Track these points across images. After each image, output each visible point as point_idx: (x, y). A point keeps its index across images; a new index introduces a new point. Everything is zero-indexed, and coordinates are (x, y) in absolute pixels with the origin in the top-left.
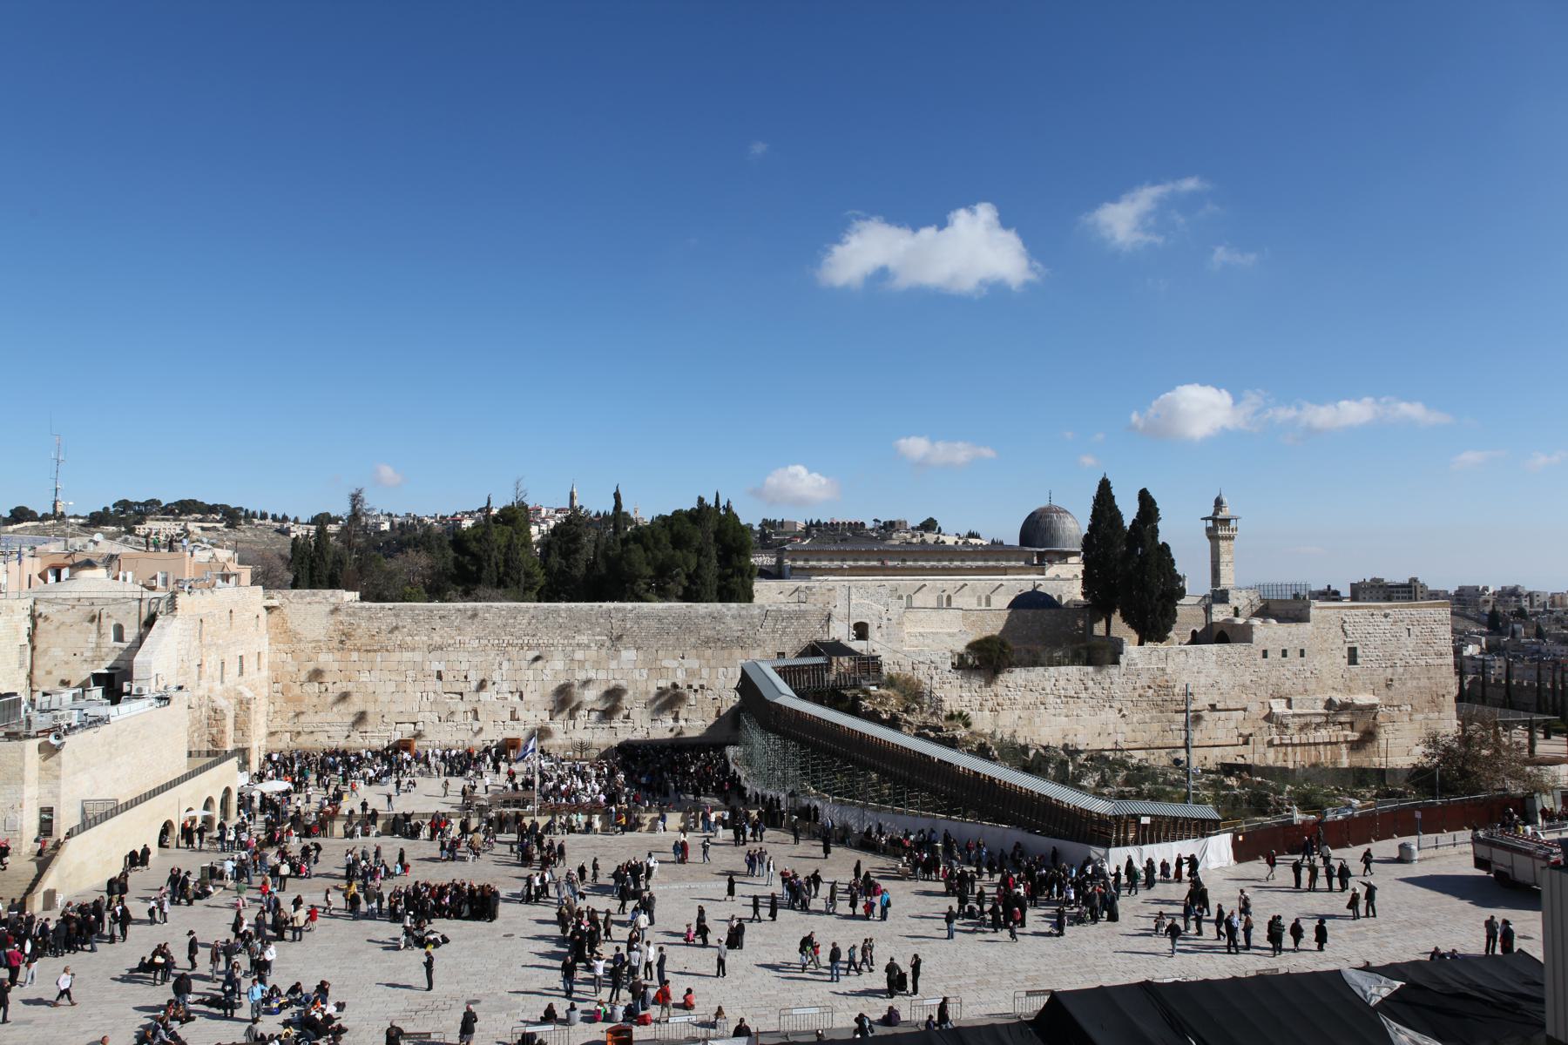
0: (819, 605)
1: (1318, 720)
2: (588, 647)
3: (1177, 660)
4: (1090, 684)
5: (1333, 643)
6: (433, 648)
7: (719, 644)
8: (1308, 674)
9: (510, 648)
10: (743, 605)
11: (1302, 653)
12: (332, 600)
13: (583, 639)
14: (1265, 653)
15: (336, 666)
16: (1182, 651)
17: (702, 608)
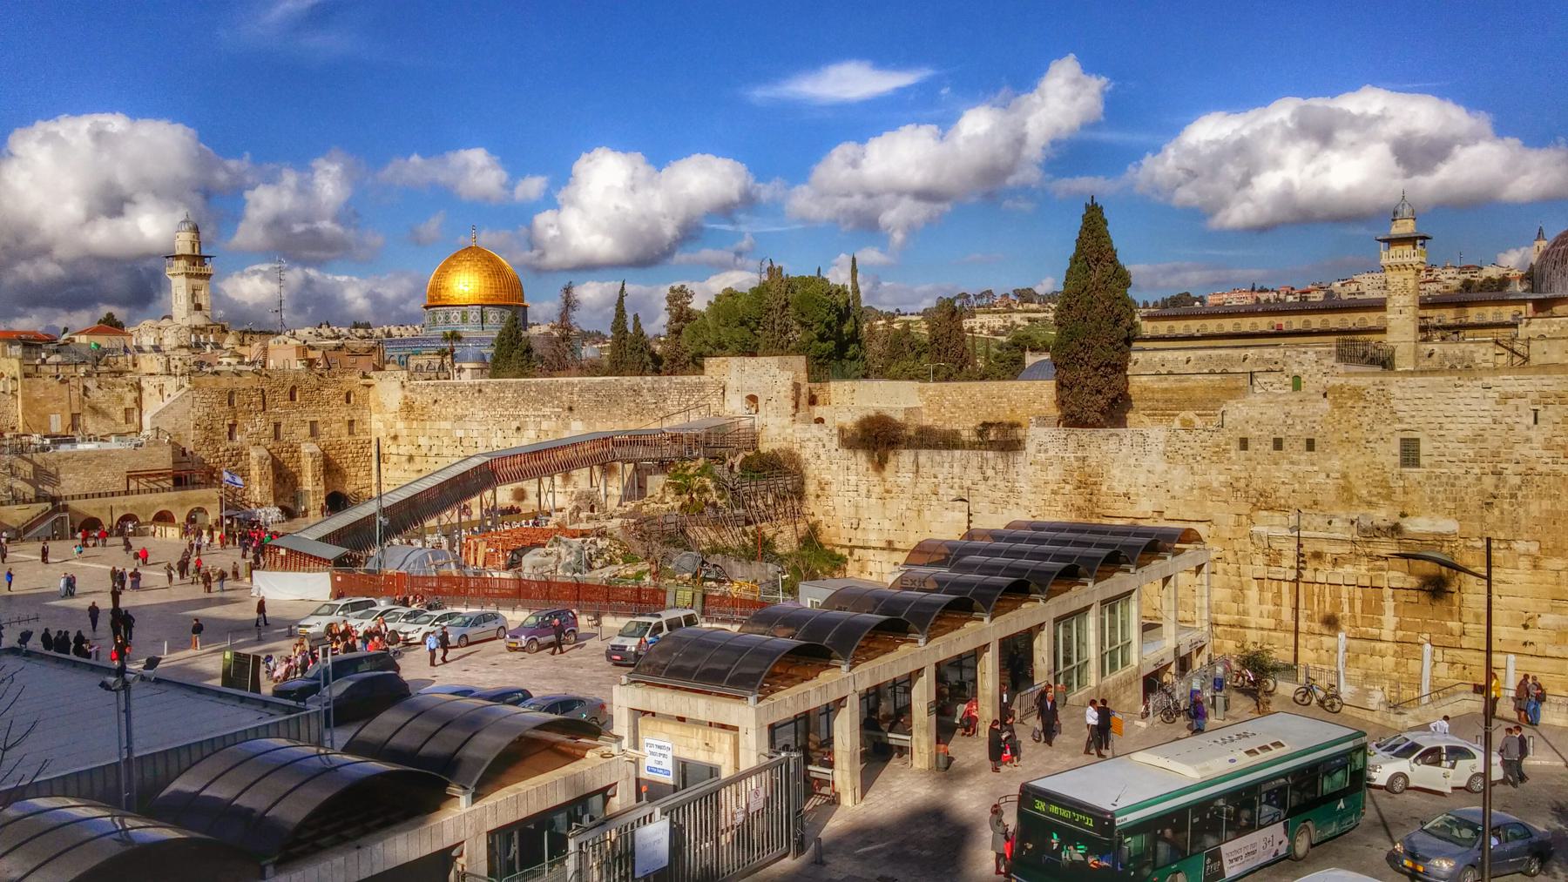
0: (715, 377)
1: (1338, 549)
2: (550, 417)
3: (1104, 448)
4: (990, 473)
5: (1372, 430)
6: (460, 418)
7: (639, 416)
8: (1321, 477)
9: (501, 419)
10: (656, 378)
11: (1310, 445)
12: (401, 379)
13: (547, 411)
14: (1244, 443)
15: (405, 432)
16: (1111, 435)
17: (627, 381)
